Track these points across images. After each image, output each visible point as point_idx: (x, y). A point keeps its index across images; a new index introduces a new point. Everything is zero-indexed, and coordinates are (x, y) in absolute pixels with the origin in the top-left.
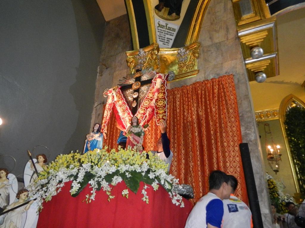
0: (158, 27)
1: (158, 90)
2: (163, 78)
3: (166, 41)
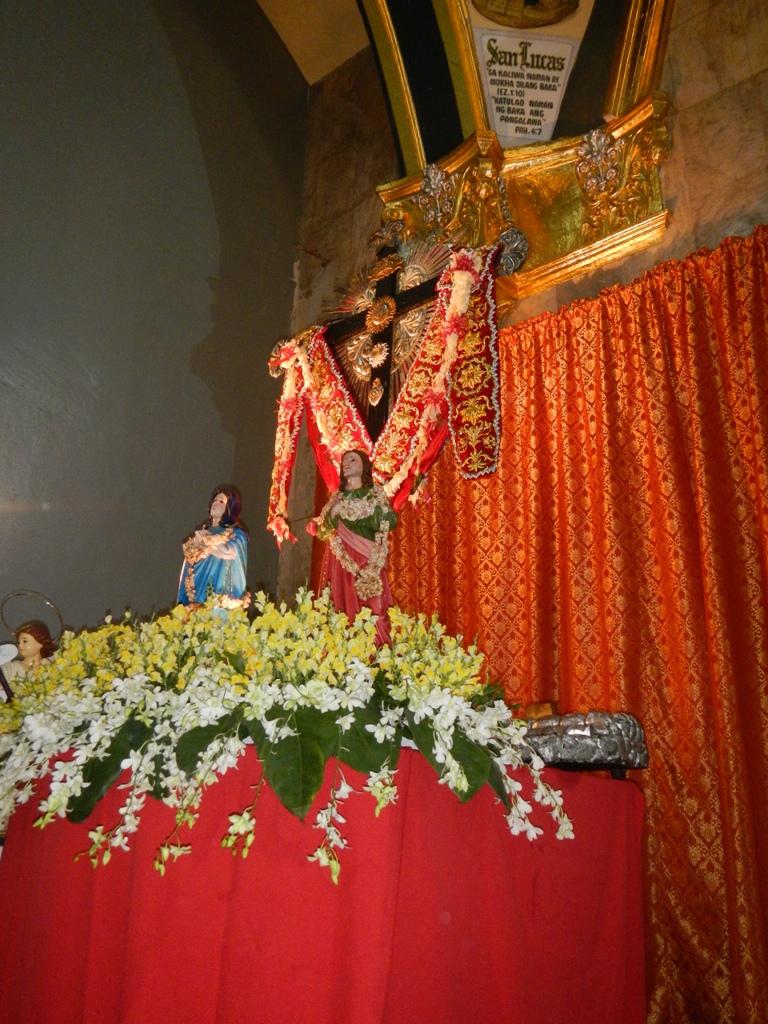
0: (492, 62)
1: (459, 325)
2: (478, 268)
3: (527, 116)
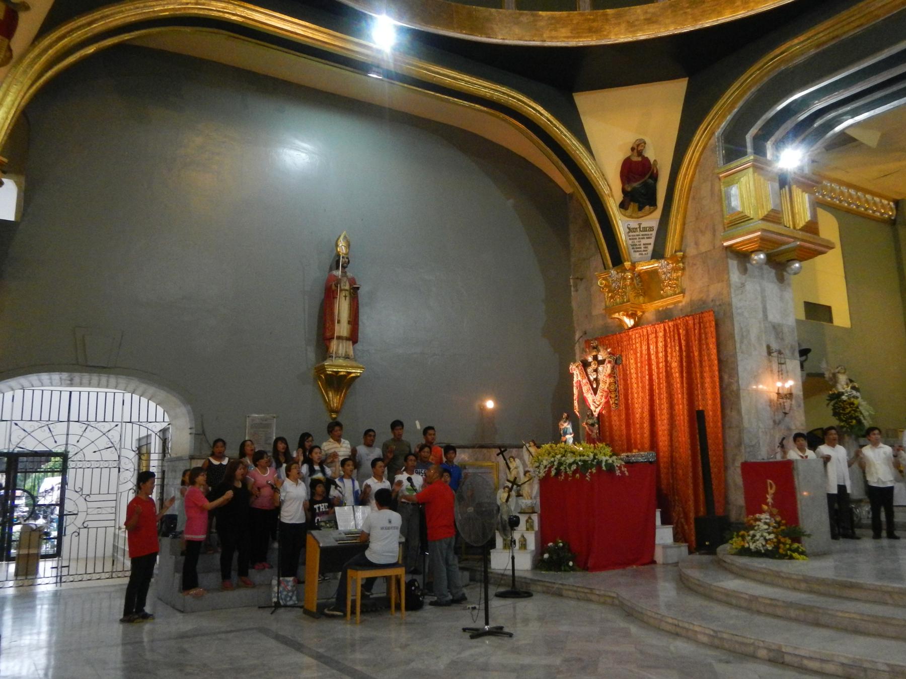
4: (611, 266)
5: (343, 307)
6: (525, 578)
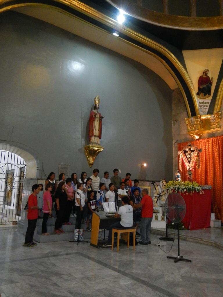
0: (199, 104)
3: (204, 110)
4: (191, 116)
5: (96, 124)
6: (162, 231)
